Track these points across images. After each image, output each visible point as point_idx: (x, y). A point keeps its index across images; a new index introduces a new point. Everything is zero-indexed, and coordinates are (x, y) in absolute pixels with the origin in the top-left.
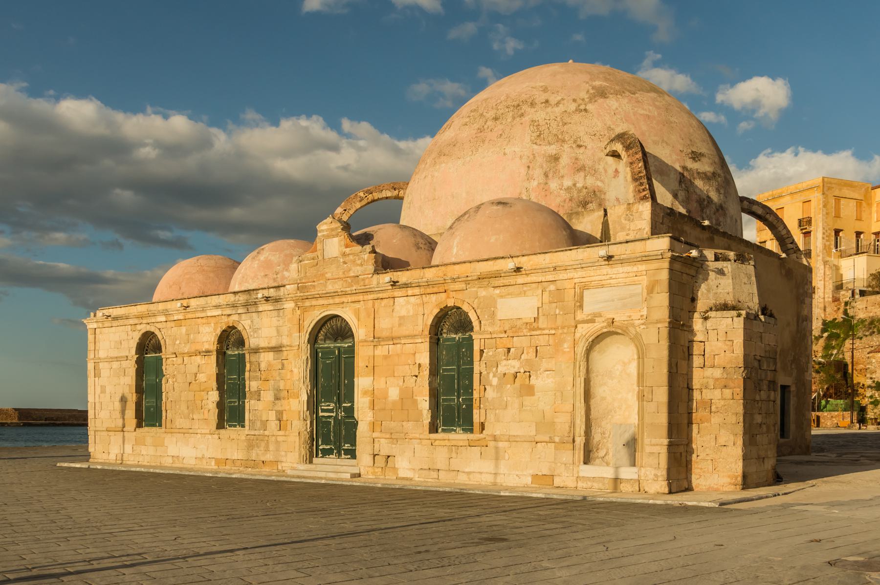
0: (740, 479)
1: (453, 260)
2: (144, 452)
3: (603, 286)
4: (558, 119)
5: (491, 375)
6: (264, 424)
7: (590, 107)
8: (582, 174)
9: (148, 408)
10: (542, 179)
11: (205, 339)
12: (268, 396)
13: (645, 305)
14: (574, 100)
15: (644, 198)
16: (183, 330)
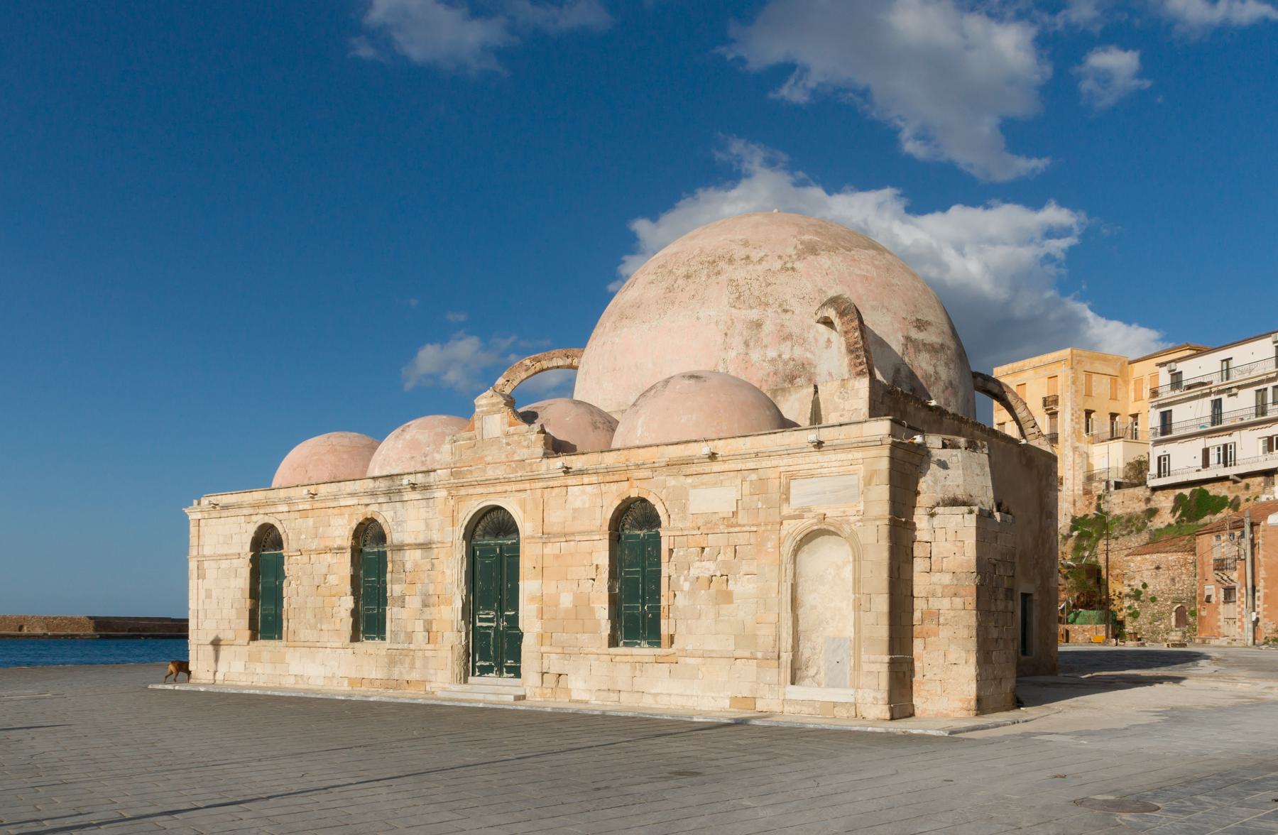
0: (973, 703)
1: (637, 443)
2: (259, 670)
3: (812, 476)
5: (682, 579)
6: (410, 636)
7: (798, 265)
8: (789, 343)
9: (266, 618)
10: (742, 349)
11: (337, 533)
12: (414, 603)
13: (861, 499)
14: (780, 257)
15: (861, 374)
16: (310, 521)
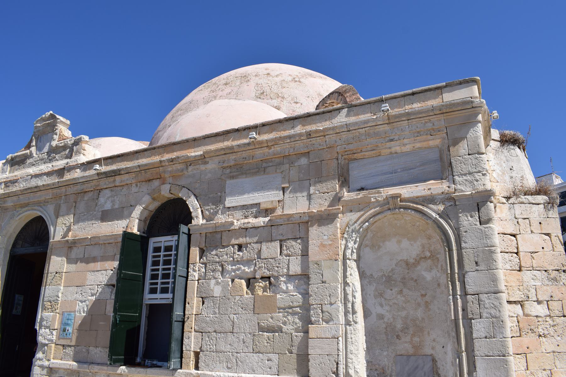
4: (278, 84)
5: (213, 282)
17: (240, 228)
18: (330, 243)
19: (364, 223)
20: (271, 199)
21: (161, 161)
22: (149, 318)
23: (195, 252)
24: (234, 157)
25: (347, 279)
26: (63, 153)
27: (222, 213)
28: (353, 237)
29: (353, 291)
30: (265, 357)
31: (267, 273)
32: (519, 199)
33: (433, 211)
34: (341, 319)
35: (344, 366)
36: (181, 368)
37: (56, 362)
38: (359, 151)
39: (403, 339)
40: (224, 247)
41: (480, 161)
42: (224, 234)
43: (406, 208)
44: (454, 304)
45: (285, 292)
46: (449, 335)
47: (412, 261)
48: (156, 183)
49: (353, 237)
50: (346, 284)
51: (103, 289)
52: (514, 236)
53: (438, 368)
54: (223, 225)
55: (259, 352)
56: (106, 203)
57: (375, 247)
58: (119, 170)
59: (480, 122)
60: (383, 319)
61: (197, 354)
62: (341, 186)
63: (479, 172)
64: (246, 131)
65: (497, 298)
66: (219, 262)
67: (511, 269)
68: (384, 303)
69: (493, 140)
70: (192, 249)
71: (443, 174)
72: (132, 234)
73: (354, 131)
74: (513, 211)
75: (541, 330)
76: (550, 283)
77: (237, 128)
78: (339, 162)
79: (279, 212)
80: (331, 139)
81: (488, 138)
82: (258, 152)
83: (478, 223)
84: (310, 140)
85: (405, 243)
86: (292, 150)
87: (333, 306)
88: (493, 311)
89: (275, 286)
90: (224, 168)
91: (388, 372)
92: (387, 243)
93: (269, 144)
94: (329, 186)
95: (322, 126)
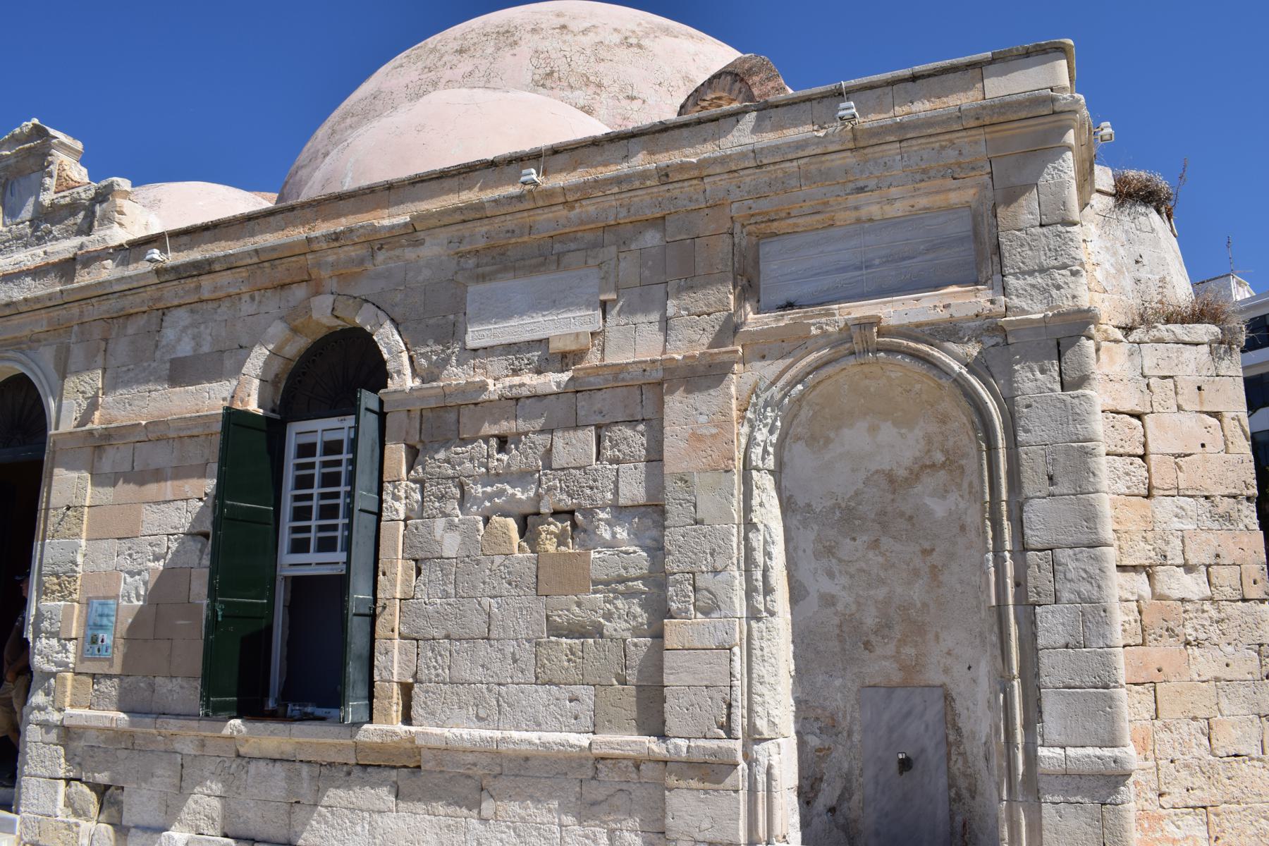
4: (588, 52)
5: (440, 523)
17: (502, 398)
18: (714, 431)
19: (792, 384)
20: (575, 329)
21: (309, 240)
22: (291, 608)
23: (396, 454)
24: (484, 229)
25: (753, 515)
26: (70, 221)
27: (460, 363)
28: (766, 418)
29: (765, 542)
30: (563, 693)
31: (567, 502)
32: (1154, 333)
33: (953, 358)
34: (737, 606)
35: (745, 712)
36: (371, 721)
37: (78, 714)
38: (783, 215)
39: (879, 651)
40: (464, 442)
41: (1066, 241)
42: (464, 411)
43: (890, 350)
44: (997, 572)
45: (609, 546)
46: (983, 641)
47: (902, 473)
48: (300, 292)
49: (766, 418)
50: (749, 525)
51: (182, 544)
52: (1138, 416)
53: (955, 715)
54: (462, 390)
55: (550, 683)
56: (179, 340)
57: (817, 440)
58: (210, 262)
59: (1069, 148)
60: (834, 605)
61: (406, 690)
62: (741, 299)
63: (1065, 267)
64: (514, 165)
65: (1096, 559)
66: (453, 478)
67: (1127, 492)
68: (836, 568)
69: (1099, 191)
70: (390, 447)
71: (979, 271)
72: (246, 414)
73: (772, 167)
74: (1137, 360)
75: (1189, 631)
76: (1216, 526)
77: (490, 157)
78: (737, 240)
79: (593, 359)
80: (716, 185)
81: (1088, 188)
82: (543, 217)
83: (1058, 387)
84: (666, 187)
85: (887, 432)
86: (623, 212)
87: (719, 577)
88: (1084, 588)
89: (585, 531)
90: (461, 255)
91: (844, 724)
92: (846, 432)
93: (569, 198)
94: (712, 299)
95: (697, 154)
